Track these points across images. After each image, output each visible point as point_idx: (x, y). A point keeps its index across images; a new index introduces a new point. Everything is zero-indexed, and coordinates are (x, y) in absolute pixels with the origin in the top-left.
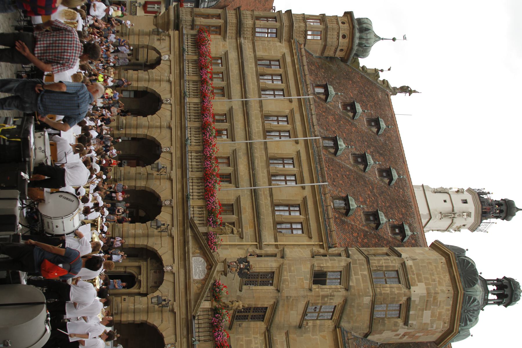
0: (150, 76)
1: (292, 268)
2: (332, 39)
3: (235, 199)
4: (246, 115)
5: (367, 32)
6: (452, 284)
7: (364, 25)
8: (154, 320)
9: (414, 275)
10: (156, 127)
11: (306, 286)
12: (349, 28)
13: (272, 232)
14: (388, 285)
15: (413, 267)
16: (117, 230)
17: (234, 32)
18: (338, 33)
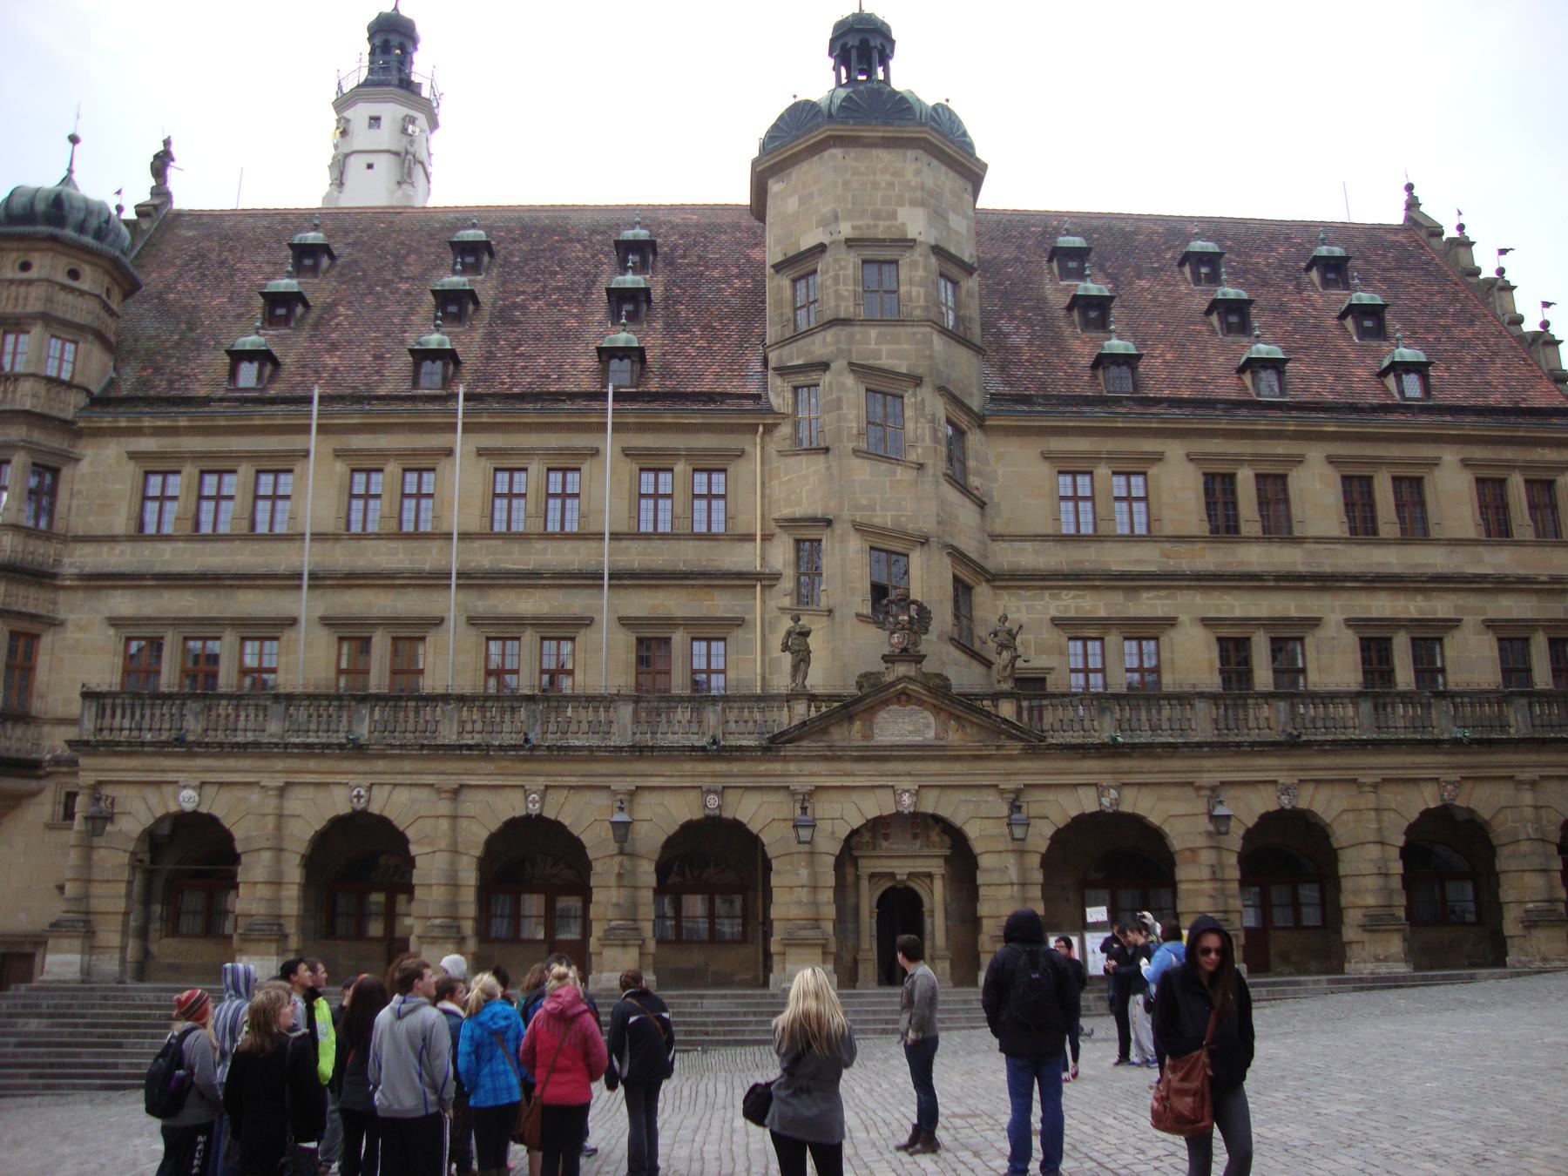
0: (265, 844)
1: (864, 502)
2: (81, 310)
3: (624, 630)
4: (352, 580)
5: (67, 205)
6: (901, 147)
7: (40, 207)
8: (1040, 837)
9: (876, 226)
10: (454, 829)
11: (910, 475)
12: (51, 254)
13: (725, 546)
14: (903, 289)
15: (860, 223)
16: (803, 933)
17: (33, 593)
18: (64, 287)
